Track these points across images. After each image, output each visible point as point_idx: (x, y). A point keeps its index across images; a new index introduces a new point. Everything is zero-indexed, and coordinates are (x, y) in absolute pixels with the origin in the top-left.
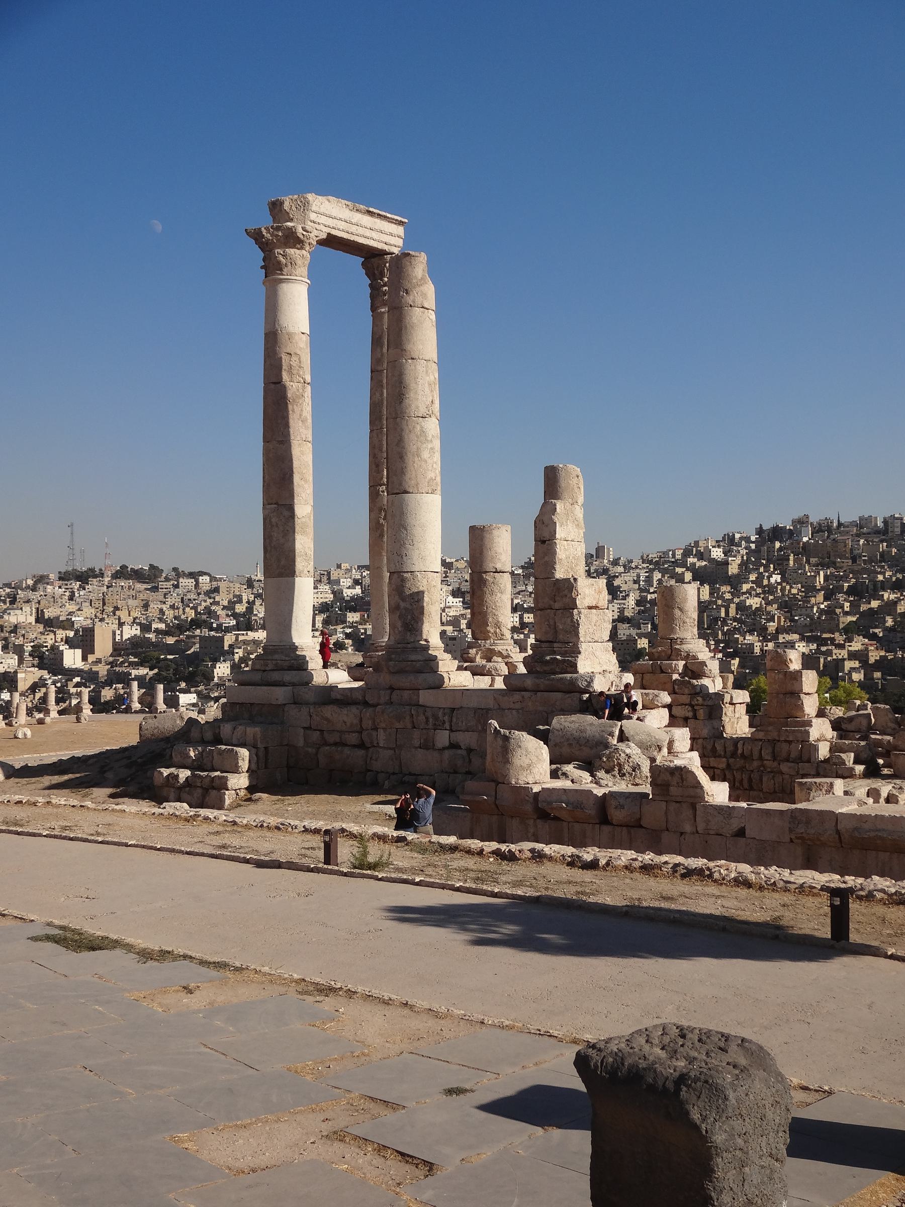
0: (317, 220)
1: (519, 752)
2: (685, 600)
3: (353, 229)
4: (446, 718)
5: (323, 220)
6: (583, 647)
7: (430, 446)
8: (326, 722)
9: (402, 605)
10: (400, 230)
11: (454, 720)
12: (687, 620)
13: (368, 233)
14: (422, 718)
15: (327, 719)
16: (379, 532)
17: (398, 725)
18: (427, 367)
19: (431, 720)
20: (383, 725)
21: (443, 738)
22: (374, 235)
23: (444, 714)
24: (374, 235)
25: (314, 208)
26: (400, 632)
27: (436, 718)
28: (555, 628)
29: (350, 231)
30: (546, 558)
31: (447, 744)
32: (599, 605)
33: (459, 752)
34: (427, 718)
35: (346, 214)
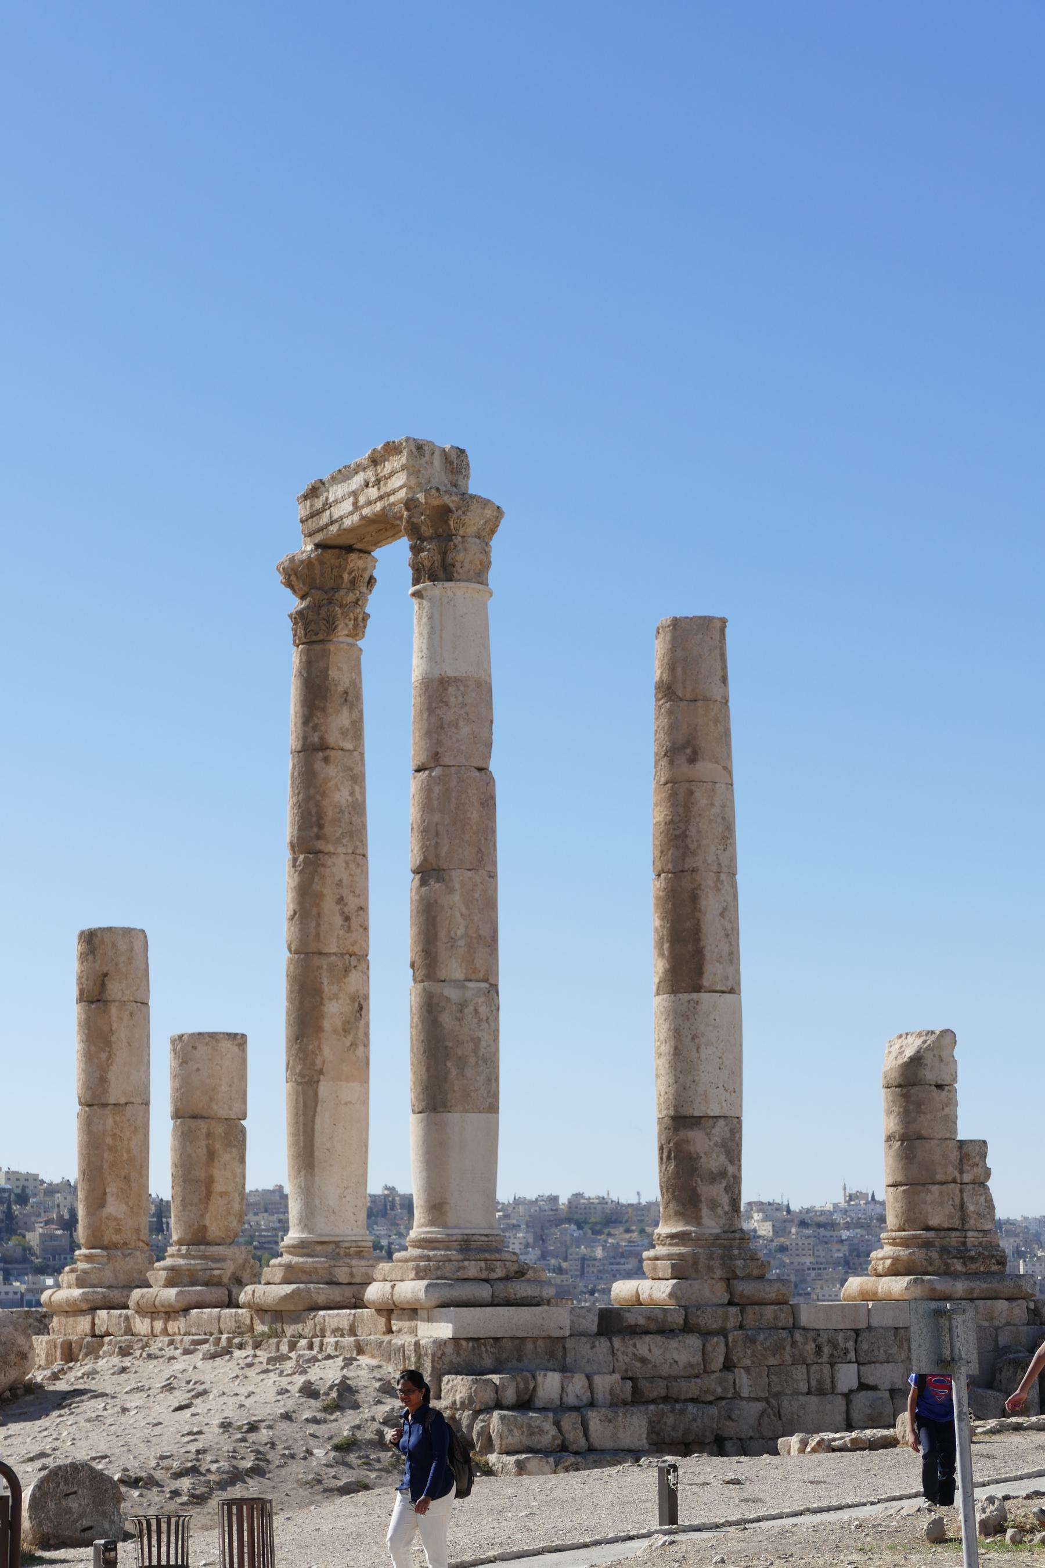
4: (850, 1345)
8: (638, 1365)
9: (731, 1169)
11: (865, 1346)
14: (811, 1347)
15: (644, 1360)
16: (350, 1038)
17: (772, 1361)
19: (826, 1350)
20: (748, 1362)
21: (847, 1376)
23: (846, 1340)
26: (726, 1213)
27: (833, 1344)
28: (962, 1206)
30: (947, 1110)
31: (855, 1385)
33: (879, 1394)
34: (819, 1349)
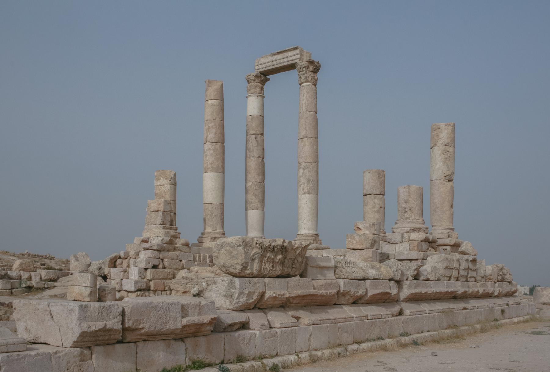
32: (160, 209)
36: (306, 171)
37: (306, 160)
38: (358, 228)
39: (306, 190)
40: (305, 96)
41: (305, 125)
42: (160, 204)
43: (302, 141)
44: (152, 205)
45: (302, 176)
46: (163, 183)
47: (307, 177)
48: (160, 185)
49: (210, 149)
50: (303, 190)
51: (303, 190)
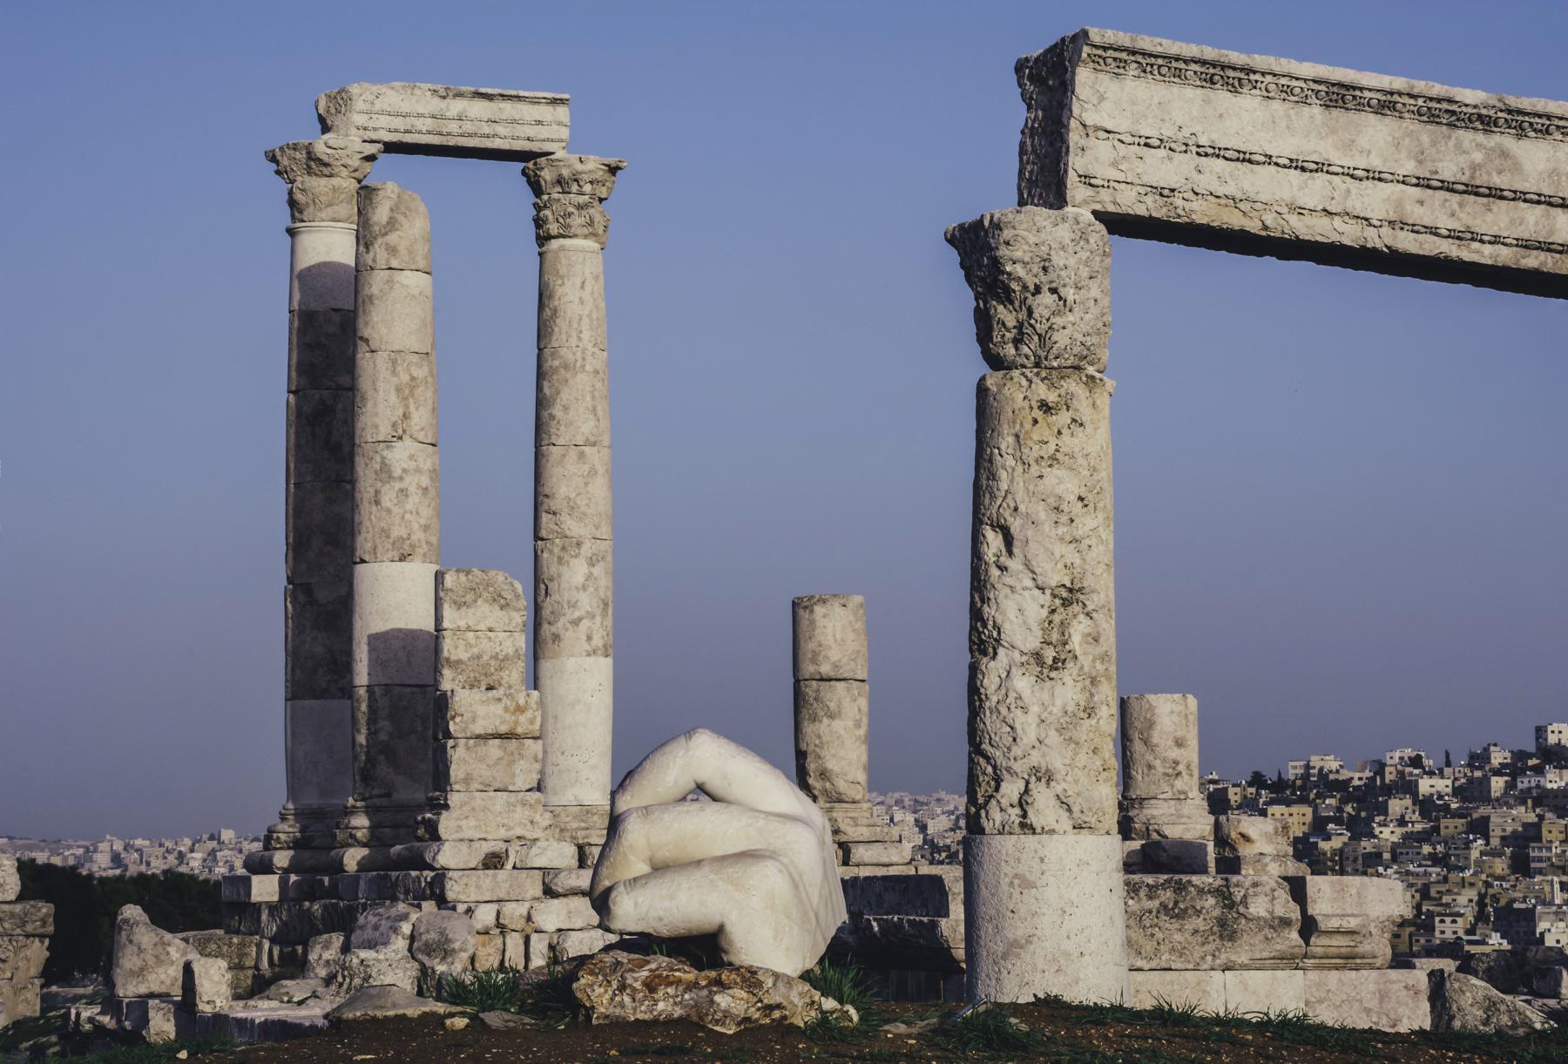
0: (370, 124)
1: (130, 949)
2: (1151, 724)
3: (453, 127)
5: (384, 121)
6: (454, 799)
7: (398, 485)
10: (562, 112)
12: (1157, 763)
13: (486, 129)
18: (394, 362)
22: (500, 129)
24: (500, 129)
25: (359, 105)
29: (445, 131)
32: (519, 730)
35: (435, 105)
36: (597, 571)
37: (597, 528)
38: (1243, 835)
39: (598, 641)
40: (588, 288)
41: (593, 398)
42: (520, 709)
43: (582, 455)
44: (482, 710)
45: (584, 588)
46: (490, 623)
47: (602, 594)
48: (469, 629)
49: (418, 470)
50: (589, 638)
51: (589, 638)
